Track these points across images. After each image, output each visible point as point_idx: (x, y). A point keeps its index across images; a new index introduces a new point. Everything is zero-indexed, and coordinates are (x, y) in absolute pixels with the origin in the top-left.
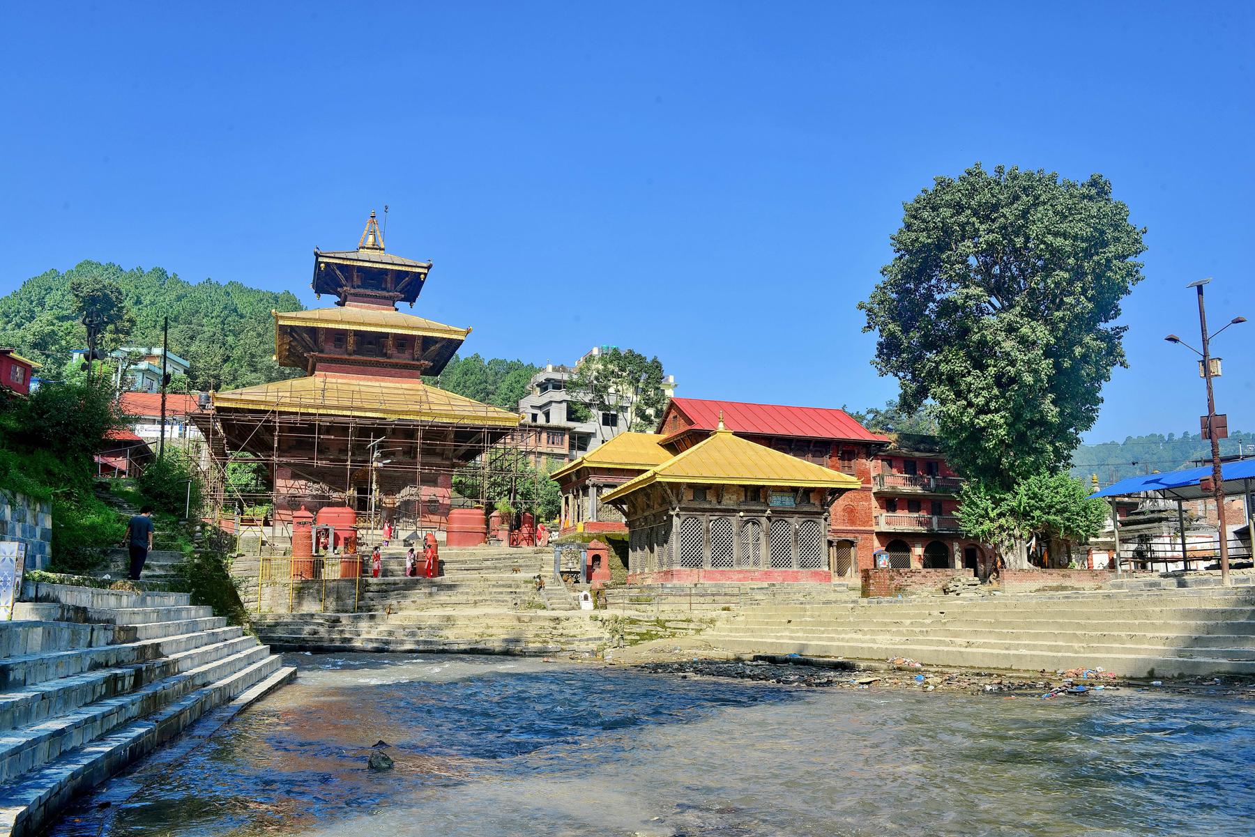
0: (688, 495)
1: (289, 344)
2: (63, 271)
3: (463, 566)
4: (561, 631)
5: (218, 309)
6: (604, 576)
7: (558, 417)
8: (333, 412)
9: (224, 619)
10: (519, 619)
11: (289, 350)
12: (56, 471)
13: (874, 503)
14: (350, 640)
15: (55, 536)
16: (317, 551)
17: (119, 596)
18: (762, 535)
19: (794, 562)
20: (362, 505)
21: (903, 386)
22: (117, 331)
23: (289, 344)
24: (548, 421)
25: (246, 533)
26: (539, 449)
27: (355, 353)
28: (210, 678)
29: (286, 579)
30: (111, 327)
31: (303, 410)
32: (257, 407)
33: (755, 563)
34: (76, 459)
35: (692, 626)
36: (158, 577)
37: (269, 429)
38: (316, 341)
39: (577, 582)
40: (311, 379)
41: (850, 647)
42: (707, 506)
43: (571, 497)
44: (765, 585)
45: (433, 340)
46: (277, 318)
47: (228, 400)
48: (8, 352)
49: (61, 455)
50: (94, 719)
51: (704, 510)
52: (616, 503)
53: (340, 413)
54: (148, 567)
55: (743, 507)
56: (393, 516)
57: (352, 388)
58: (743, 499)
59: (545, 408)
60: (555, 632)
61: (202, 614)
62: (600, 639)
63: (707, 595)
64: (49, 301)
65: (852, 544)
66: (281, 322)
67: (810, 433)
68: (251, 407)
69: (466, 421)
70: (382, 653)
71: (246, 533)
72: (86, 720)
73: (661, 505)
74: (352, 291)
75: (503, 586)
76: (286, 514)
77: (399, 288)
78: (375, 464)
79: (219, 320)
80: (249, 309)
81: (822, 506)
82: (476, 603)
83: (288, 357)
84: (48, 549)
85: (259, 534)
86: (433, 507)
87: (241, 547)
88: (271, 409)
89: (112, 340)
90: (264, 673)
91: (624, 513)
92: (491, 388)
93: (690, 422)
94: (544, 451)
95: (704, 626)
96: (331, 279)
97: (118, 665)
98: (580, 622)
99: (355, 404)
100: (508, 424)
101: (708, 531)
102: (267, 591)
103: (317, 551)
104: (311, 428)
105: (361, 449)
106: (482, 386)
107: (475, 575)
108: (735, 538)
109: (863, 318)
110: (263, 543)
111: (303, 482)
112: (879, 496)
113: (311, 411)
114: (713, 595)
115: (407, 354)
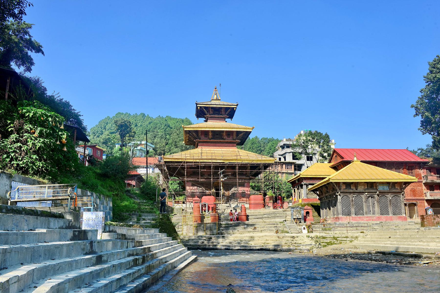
0: (344, 187)
1: (189, 137)
2: (111, 117)
3: (256, 217)
4: (295, 242)
5: (163, 126)
6: (311, 220)
7: (289, 159)
9: (171, 238)
10: (278, 237)
11: (188, 139)
12: (113, 186)
13: (424, 187)
14: (216, 245)
15: (114, 209)
16: (202, 212)
17: (136, 230)
18: (375, 202)
19: (390, 213)
20: (217, 195)
21: (433, 138)
22: (130, 136)
23: (189, 137)
24: (285, 160)
25: (177, 207)
26: (283, 171)
28: (168, 259)
29: (191, 223)
30: (128, 135)
31: (195, 161)
32: (179, 161)
33: (373, 214)
34: (119, 182)
35: (348, 239)
36: (148, 223)
37: (183, 168)
38: (198, 135)
39: (300, 222)
40: (197, 149)
41: (418, 248)
42: (351, 191)
43: (296, 189)
44: (378, 222)
46: (184, 128)
47: (168, 158)
48: (95, 146)
50: (130, 274)
51: (350, 193)
52: (314, 191)
53: (208, 161)
54: (144, 219)
55: (367, 191)
56: (228, 199)
57: (212, 152)
58: (366, 187)
59: (284, 155)
60: (293, 242)
61: (163, 236)
62: (311, 245)
63: (354, 227)
64: (107, 127)
65: (415, 205)
66: (185, 129)
67: (394, 160)
68: (176, 160)
69: (254, 162)
70: (228, 250)
71: (177, 207)
72: (128, 275)
73: (332, 191)
74: (210, 116)
75: (272, 224)
76: (190, 199)
77: (227, 113)
78: (221, 180)
79: (164, 130)
80: (174, 125)
81: (401, 189)
82: (261, 231)
83: (188, 142)
84: (111, 214)
85: (181, 207)
86: (243, 195)
87: (175, 212)
88: (183, 161)
90: (186, 258)
91: (317, 194)
92: (262, 149)
93: (342, 158)
94: (285, 172)
95: (353, 239)
96: (202, 112)
97: (137, 255)
98: (302, 238)
99: (213, 158)
100: (270, 162)
101: (352, 201)
102: (185, 228)
103: (202, 212)
104: (198, 167)
105: (216, 174)
106: (259, 148)
107: (261, 220)
108: (364, 204)
109: (414, 111)
110: (183, 210)
111: (196, 187)
112: (426, 184)
113: (197, 161)
114: (356, 227)
115: (231, 138)
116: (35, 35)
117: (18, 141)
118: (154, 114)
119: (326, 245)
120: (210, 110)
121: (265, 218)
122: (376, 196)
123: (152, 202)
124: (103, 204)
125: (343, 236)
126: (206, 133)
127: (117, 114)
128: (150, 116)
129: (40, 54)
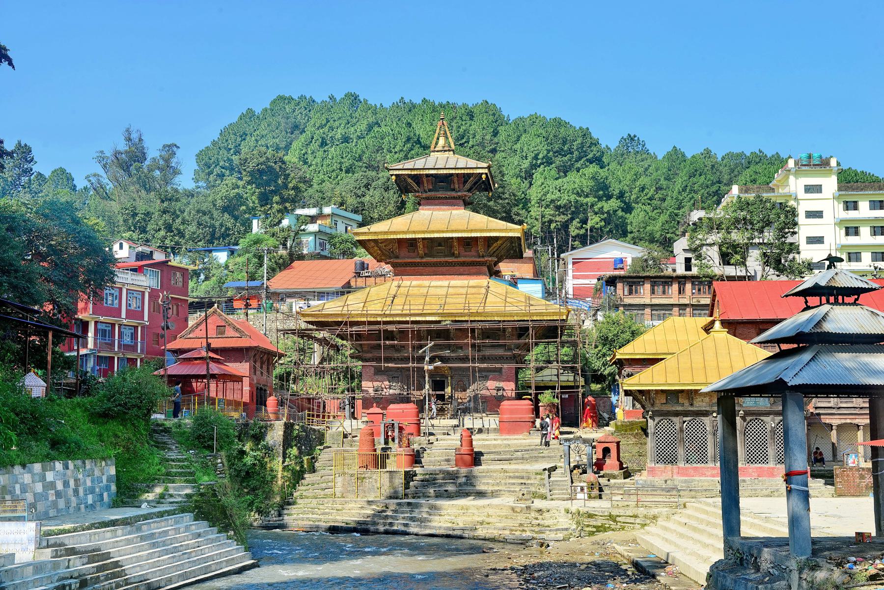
2: (258, 110)
5: (400, 143)
8: (398, 319)
9: (215, 529)
12: (120, 434)
14: (391, 524)
15: (118, 479)
27: (426, 255)
30: (276, 198)
35: (638, 521)
42: (680, 408)
47: (312, 315)
48: (167, 262)
49: (123, 422)
51: (677, 414)
53: (404, 319)
62: (567, 529)
66: (358, 238)
75: (517, 477)
77: (468, 186)
84: (113, 488)
87: (328, 441)
89: (279, 211)
95: (648, 522)
101: (681, 430)
102: (339, 480)
106: (715, 188)
110: (345, 436)
113: (379, 319)
115: (473, 253)
118: (381, 95)
119: (594, 532)
120: (425, 180)
121: (516, 459)
123: (207, 453)
124: (91, 474)
125: (627, 514)
127: (273, 102)
128: (371, 102)
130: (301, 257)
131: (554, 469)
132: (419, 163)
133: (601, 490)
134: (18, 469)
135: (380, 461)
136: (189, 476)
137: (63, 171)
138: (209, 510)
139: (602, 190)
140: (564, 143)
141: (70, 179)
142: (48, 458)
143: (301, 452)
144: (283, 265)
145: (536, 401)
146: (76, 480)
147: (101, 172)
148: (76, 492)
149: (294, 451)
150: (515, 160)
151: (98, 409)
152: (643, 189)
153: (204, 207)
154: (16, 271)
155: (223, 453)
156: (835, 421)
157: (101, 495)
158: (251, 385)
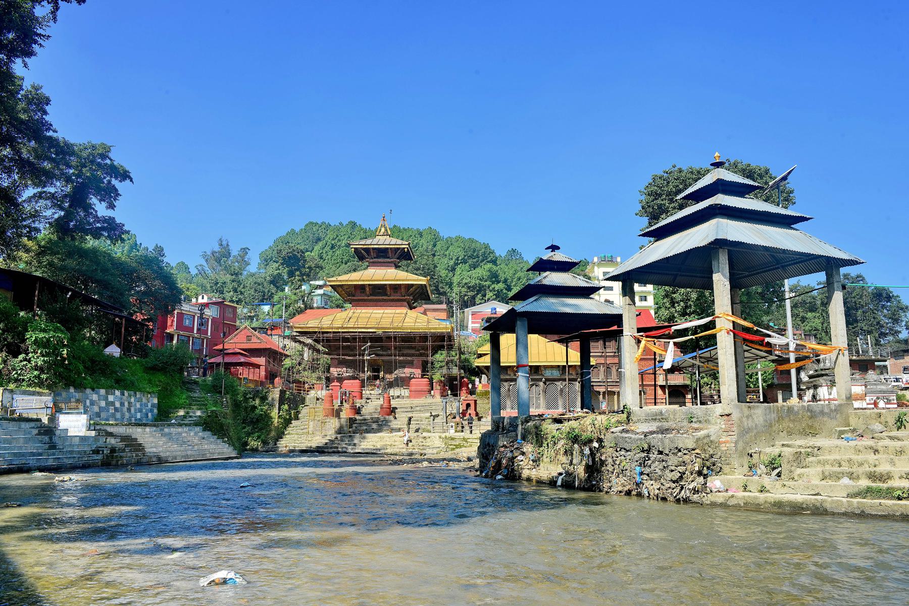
2: (297, 230)
15: (159, 406)
27: (371, 295)
30: (298, 273)
45: (412, 285)
84: (156, 411)
87: (307, 402)
101: (509, 390)
102: (311, 423)
110: (318, 399)
116: (118, 158)
117: (25, 360)
122: (541, 384)
124: (140, 400)
126: (361, 288)
127: (307, 225)
128: (364, 226)
129: (128, 181)
130: (312, 308)
131: (438, 416)
132: (369, 242)
133: (463, 427)
134: (88, 391)
135: (337, 413)
136: (202, 406)
137: (183, 263)
138: (212, 425)
139: (494, 277)
140: (474, 251)
141: (187, 268)
142: (110, 389)
143: (290, 408)
144: (300, 311)
145: (431, 380)
146: (129, 403)
147: (205, 264)
148: (129, 410)
149: (286, 407)
150: (445, 260)
151: (150, 365)
152: (519, 279)
153: (259, 280)
154: (113, 288)
155: (228, 396)
156: (602, 390)
157: (147, 415)
158: (266, 371)
